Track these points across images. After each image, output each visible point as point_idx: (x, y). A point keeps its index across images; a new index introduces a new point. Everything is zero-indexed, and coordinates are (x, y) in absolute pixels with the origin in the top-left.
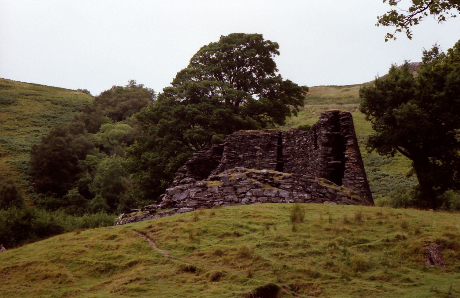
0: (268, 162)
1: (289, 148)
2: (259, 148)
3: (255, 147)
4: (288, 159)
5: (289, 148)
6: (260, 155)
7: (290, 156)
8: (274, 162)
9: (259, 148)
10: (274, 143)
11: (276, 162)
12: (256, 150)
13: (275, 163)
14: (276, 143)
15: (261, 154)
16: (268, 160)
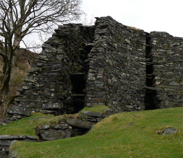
0: (138, 60)
1: (162, 50)
2: (129, 42)
3: (126, 40)
4: (159, 61)
5: (162, 50)
6: (130, 50)
7: (161, 59)
8: (143, 61)
9: (129, 42)
10: (142, 41)
11: (145, 62)
12: (127, 43)
13: (144, 63)
14: (144, 42)
15: (131, 49)
16: (137, 58)
